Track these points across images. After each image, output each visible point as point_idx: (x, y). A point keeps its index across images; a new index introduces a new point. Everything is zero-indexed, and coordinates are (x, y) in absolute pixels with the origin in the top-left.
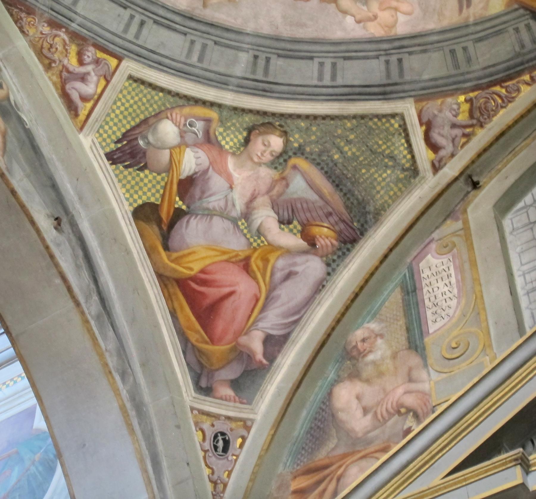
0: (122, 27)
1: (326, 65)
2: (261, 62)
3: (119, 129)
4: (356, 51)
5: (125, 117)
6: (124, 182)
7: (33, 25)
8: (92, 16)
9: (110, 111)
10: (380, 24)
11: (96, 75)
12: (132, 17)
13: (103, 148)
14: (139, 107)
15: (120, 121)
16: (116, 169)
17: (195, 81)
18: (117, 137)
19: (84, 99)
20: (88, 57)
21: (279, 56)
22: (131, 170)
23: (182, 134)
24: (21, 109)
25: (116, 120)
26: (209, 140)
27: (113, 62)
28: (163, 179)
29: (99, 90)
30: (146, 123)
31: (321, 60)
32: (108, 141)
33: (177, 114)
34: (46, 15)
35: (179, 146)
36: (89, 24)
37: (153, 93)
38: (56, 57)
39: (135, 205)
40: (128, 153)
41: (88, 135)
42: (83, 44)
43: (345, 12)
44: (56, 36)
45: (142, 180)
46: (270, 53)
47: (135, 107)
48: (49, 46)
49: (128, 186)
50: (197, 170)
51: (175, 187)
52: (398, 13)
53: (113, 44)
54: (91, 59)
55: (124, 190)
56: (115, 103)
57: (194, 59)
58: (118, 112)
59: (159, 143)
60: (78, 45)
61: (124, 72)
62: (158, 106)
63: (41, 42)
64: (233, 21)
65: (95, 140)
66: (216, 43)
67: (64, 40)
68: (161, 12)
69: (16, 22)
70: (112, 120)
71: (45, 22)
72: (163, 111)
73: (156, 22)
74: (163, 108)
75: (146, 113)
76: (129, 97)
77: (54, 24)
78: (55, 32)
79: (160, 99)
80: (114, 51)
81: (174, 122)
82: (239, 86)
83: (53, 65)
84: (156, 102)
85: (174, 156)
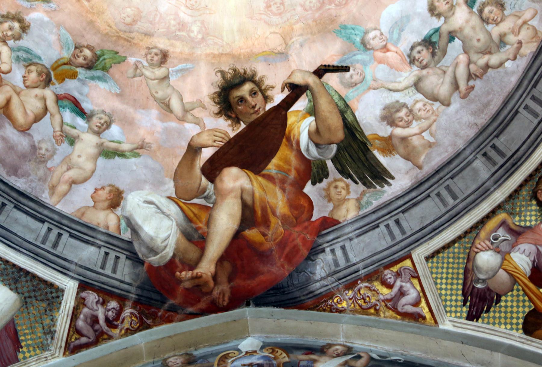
0: (388, 238)
1: (528, 105)
2: (492, 153)
3: (457, 295)
4: (535, 74)
5: (452, 284)
6: (497, 321)
7: (341, 301)
8: (366, 254)
9: (439, 292)
10: (528, 43)
11: (407, 282)
12: (387, 226)
13: (460, 317)
14: (453, 268)
15: (451, 289)
16: (483, 321)
17: (466, 212)
18: (461, 301)
19: (416, 304)
20: (390, 278)
21: (497, 136)
22: (492, 309)
23: (497, 251)
24: (388, 355)
25: (449, 292)
26: (517, 233)
27: (407, 263)
28: (518, 290)
29: (419, 288)
30: (469, 271)
31: (523, 106)
32: (459, 309)
33: (479, 244)
34: (340, 286)
35: (504, 259)
36: (369, 261)
37: (451, 249)
38: (373, 301)
39: (521, 326)
40: (479, 301)
41: (444, 321)
42: (379, 276)
43: (501, 64)
44: (359, 291)
45: (506, 307)
46: (490, 141)
47: (450, 271)
48: (362, 300)
49: (503, 321)
50: (533, 259)
51: (531, 285)
52: (529, 23)
53: (395, 254)
54: (392, 277)
55: (503, 326)
56: (436, 284)
57: (451, 202)
58: (444, 286)
59: (490, 273)
60: (377, 279)
61: (420, 260)
62: (463, 253)
63: (355, 303)
64: (446, 154)
65: (451, 319)
66: (452, 178)
67: (366, 287)
68: (400, 202)
69: (331, 311)
70: (446, 295)
71: (344, 291)
72: (469, 252)
73: (403, 212)
74: (468, 251)
75: (461, 266)
76: (440, 270)
77: (351, 286)
78: (356, 289)
79: (459, 248)
80: (401, 257)
81: (484, 249)
82: (496, 183)
83: (378, 308)
84: (459, 253)
85: (508, 268)
